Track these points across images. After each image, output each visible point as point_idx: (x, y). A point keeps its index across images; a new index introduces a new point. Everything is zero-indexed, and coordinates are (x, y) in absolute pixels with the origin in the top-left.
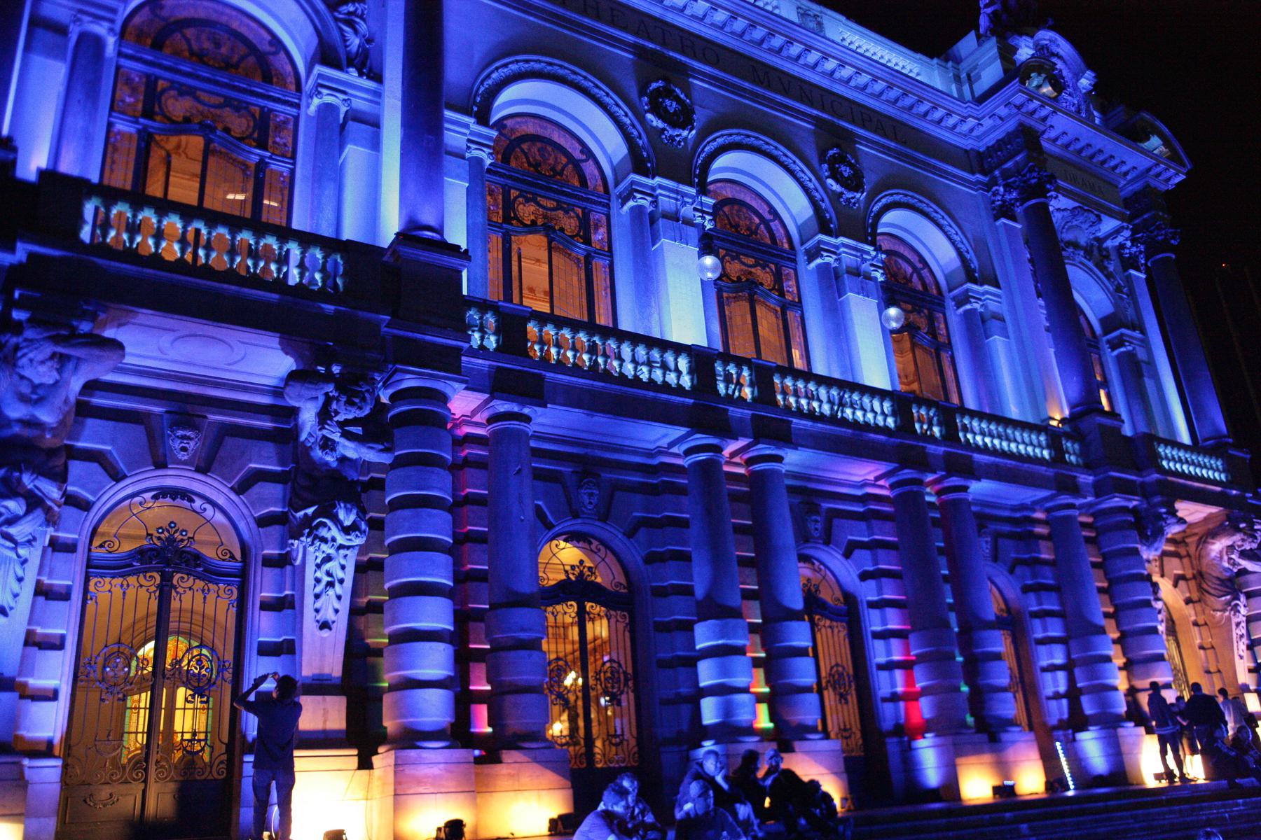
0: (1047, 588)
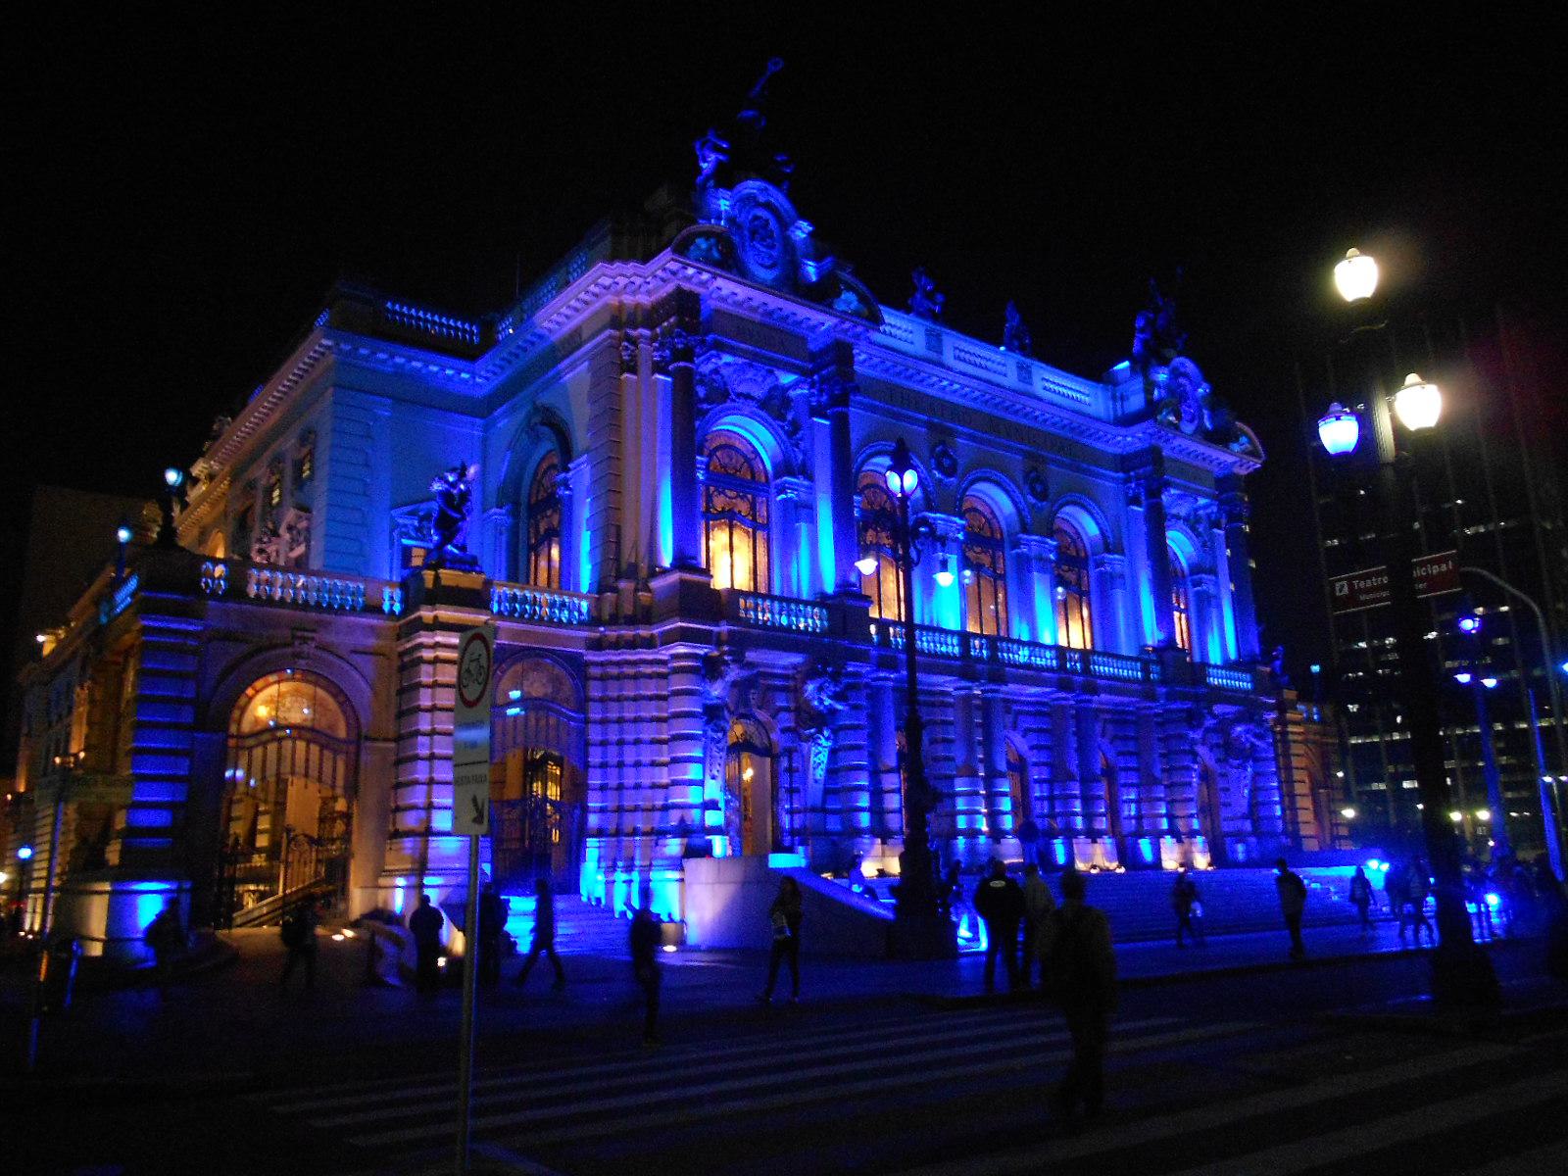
0: (1131, 754)
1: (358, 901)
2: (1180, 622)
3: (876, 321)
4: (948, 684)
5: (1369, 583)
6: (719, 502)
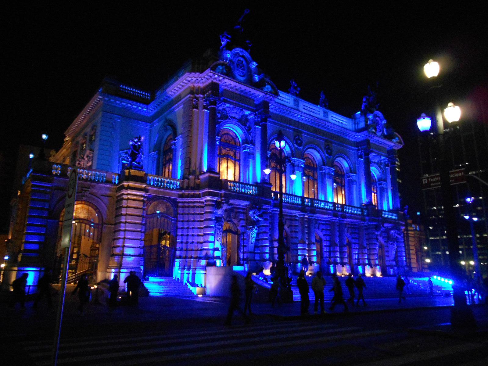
0: (357, 238)
1: (100, 276)
2: (374, 196)
3: (277, 95)
4: (297, 213)
5: (434, 180)
6: (224, 152)
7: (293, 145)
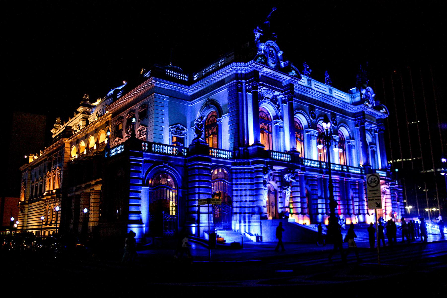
3: (300, 78)
4: (316, 175)
7: (309, 118)
